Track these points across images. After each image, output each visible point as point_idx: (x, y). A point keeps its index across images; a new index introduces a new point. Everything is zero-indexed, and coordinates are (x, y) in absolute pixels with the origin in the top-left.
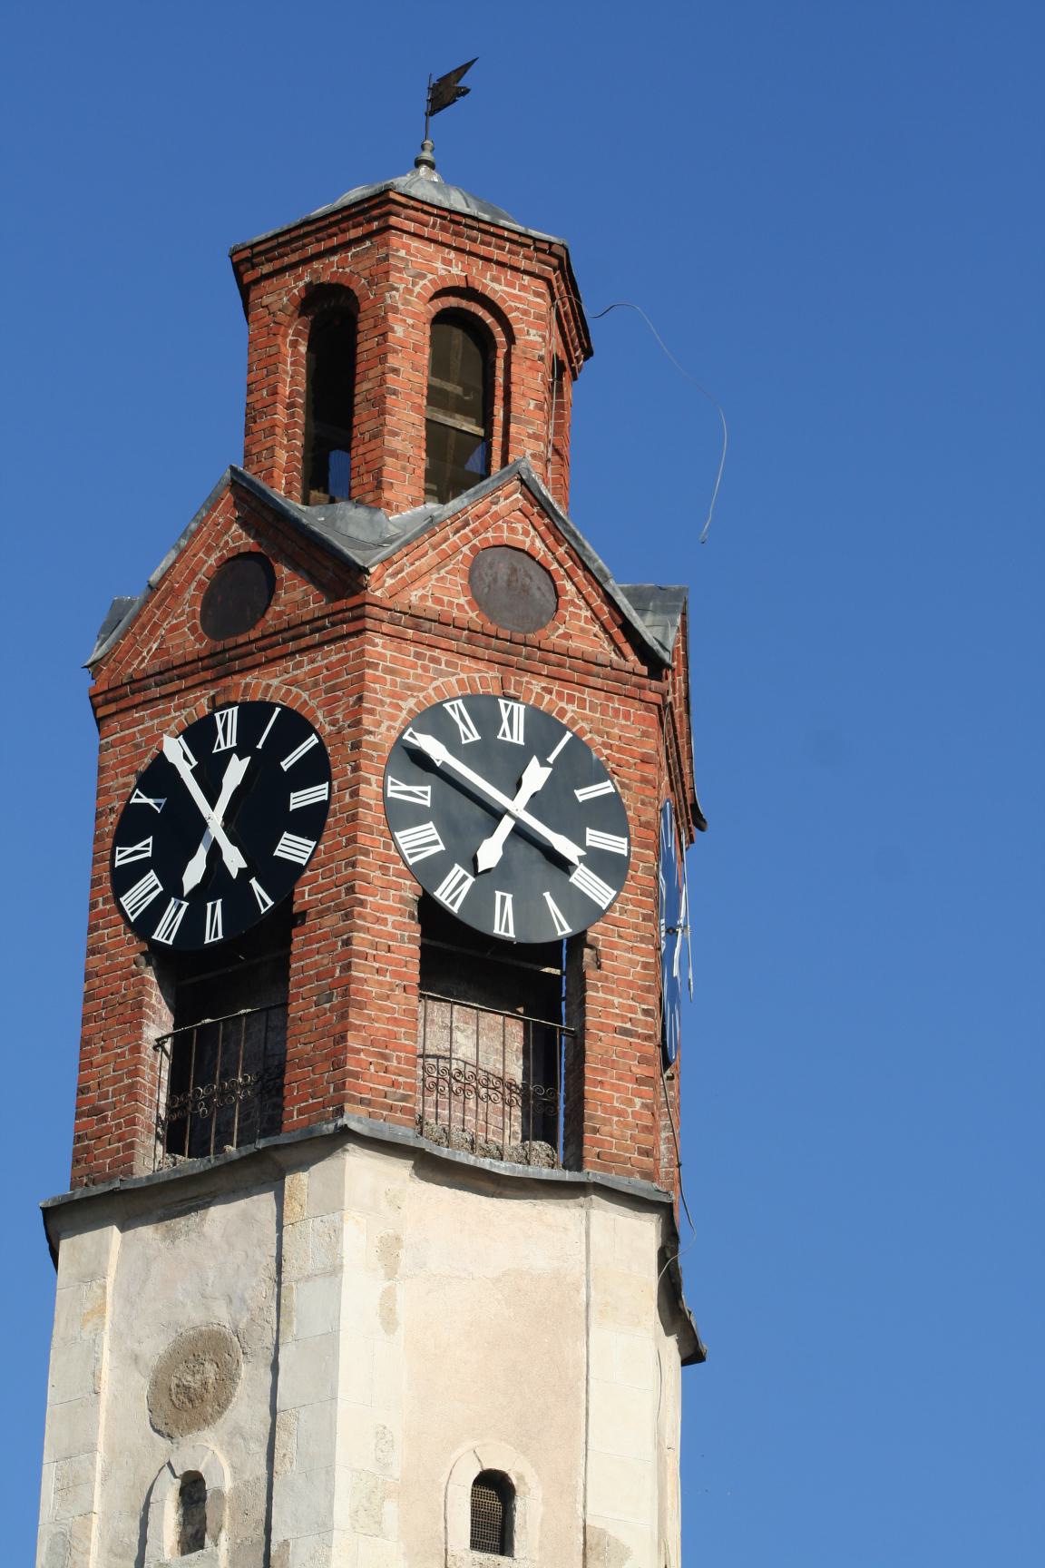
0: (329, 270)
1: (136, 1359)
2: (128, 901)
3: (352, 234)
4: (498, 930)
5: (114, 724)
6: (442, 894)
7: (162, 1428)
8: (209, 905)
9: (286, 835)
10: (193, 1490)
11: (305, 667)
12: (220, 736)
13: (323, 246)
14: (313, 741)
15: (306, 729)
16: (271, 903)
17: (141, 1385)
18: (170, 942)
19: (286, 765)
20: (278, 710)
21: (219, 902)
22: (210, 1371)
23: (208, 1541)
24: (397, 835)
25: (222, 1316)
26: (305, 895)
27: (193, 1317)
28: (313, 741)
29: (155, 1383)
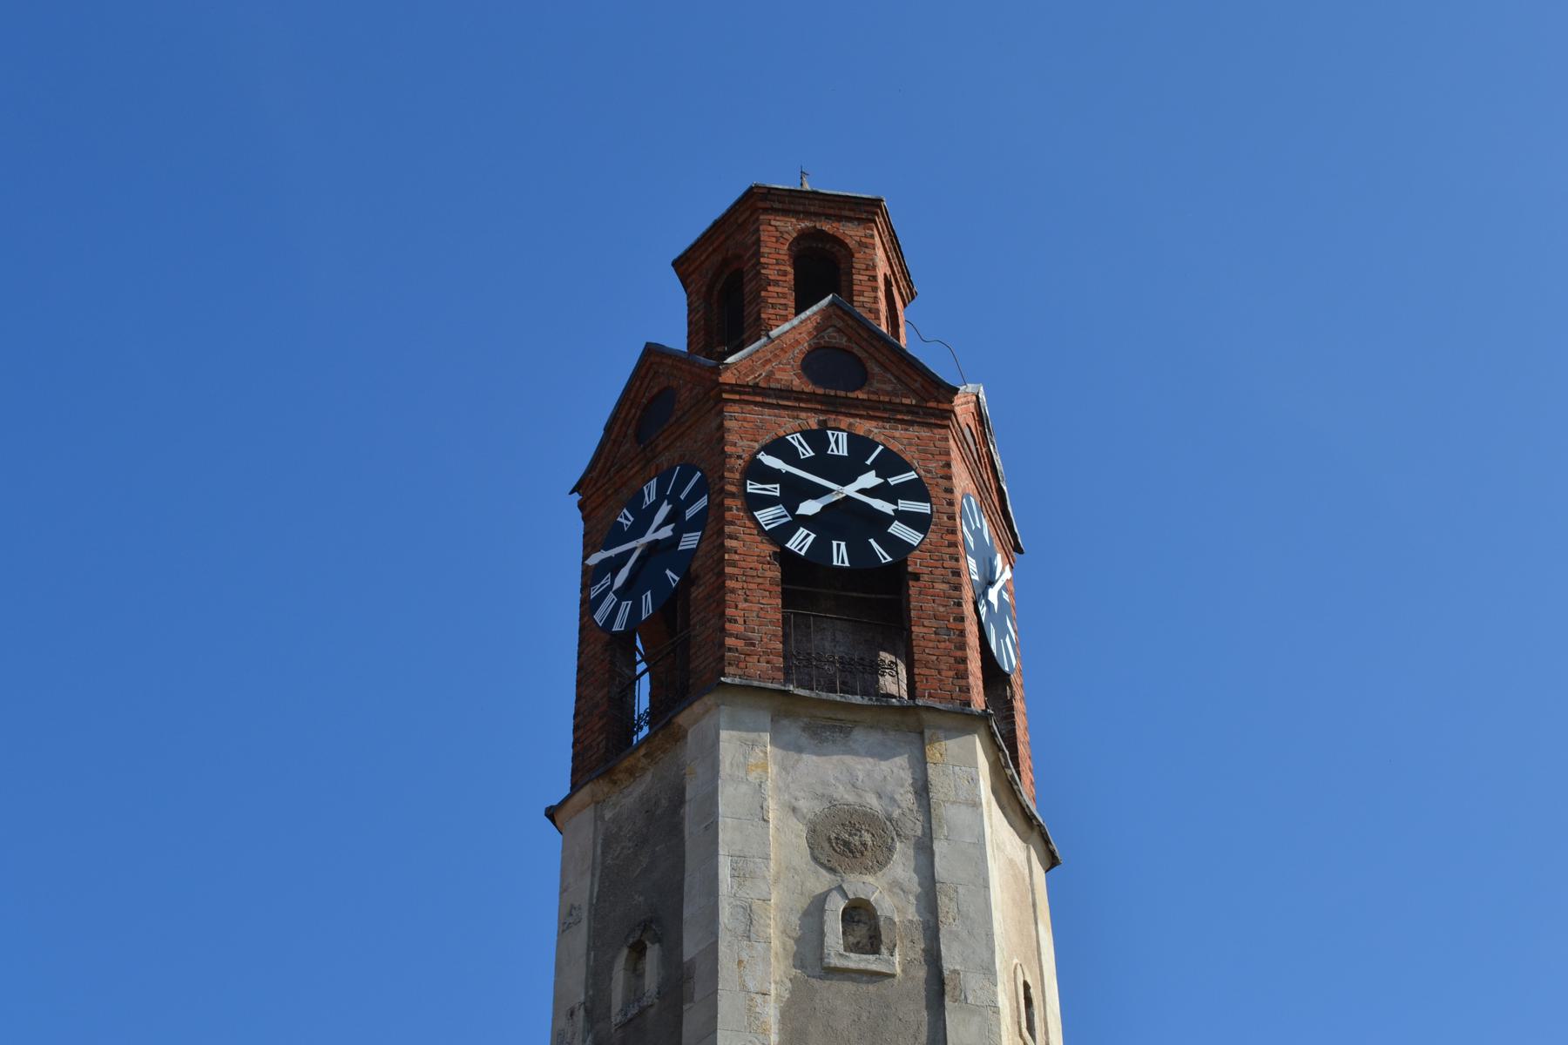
0: (827, 227)
1: (794, 810)
2: (765, 516)
3: (846, 213)
5: (736, 408)
7: (824, 860)
8: (835, 543)
10: (859, 914)
11: (916, 432)
12: (833, 445)
13: (820, 210)
14: (912, 475)
15: (906, 467)
17: (802, 829)
18: (803, 553)
21: (843, 544)
22: (867, 837)
23: (883, 949)
25: (873, 802)
27: (845, 795)
29: (813, 832)
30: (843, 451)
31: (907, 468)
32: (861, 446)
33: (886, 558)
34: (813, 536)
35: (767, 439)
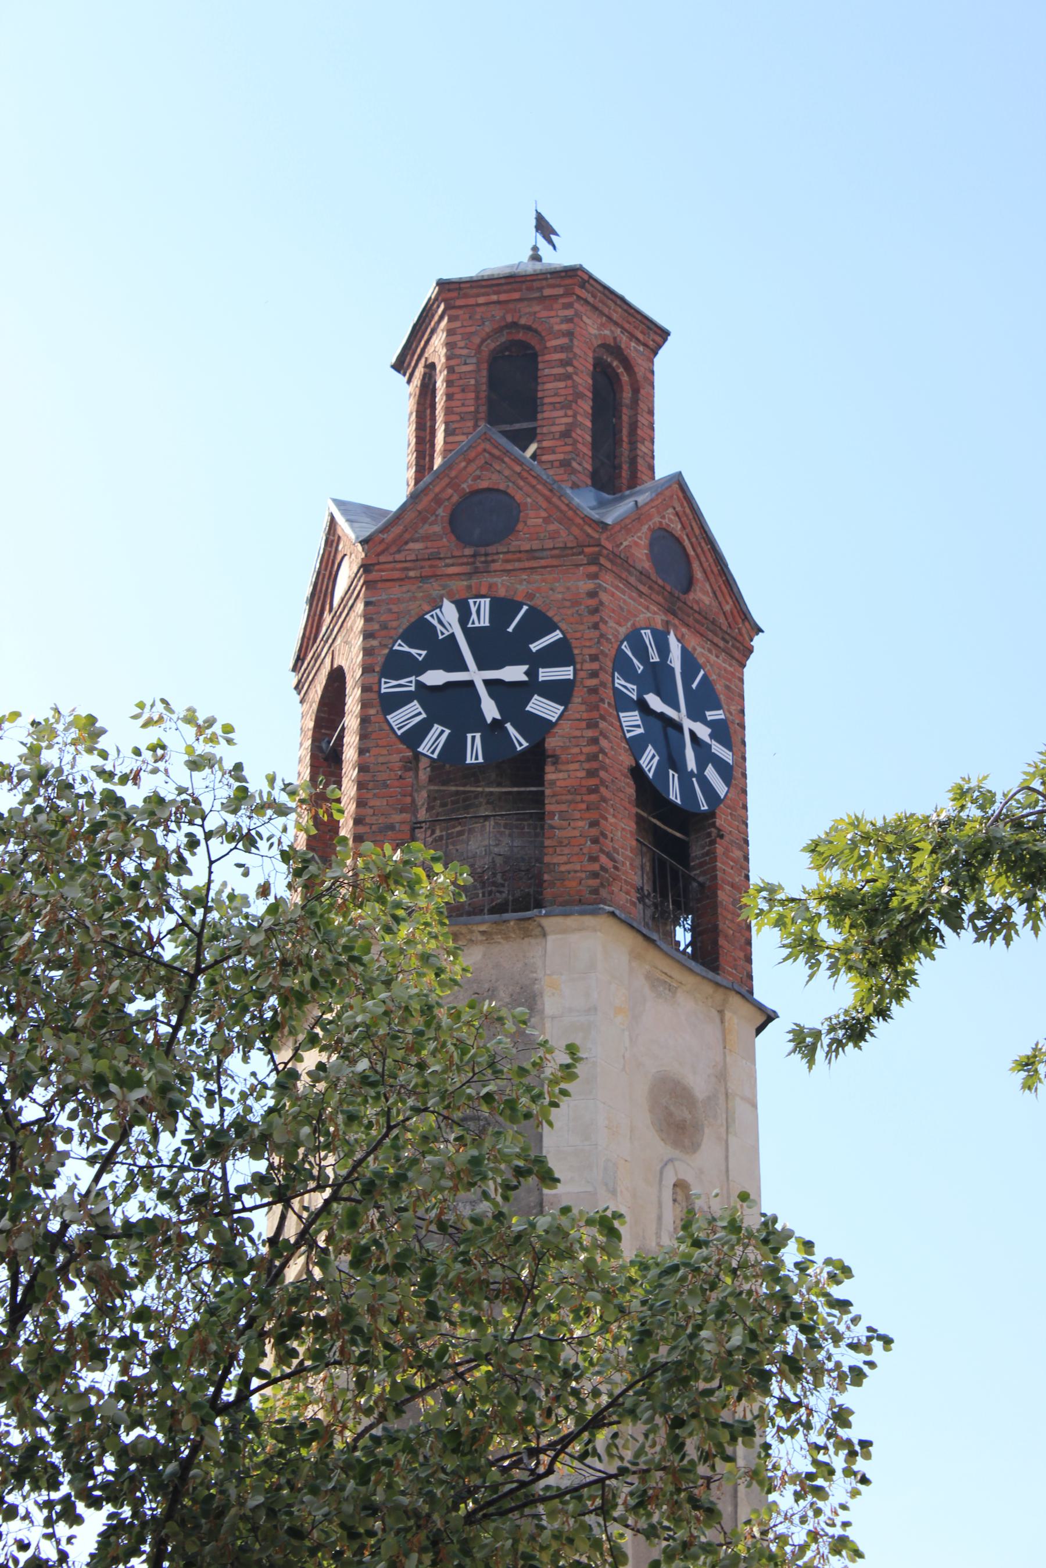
4: (672, 797)
6: (644, 762)
8: (469, 736)
9: (536, 696)
12: (474, 616)
14: (557, 635)
16: (525, 744)
19: (534, 647)
20: (525, 608)
21: (478, 735)
24: (621, 715)
26: (552, 743)
28: (557, 635)
30: (485, 622)
31: (552, 627)
32: (502, 609)
33: (521, 743)
34: (447, 732)
35: (405, 623)
